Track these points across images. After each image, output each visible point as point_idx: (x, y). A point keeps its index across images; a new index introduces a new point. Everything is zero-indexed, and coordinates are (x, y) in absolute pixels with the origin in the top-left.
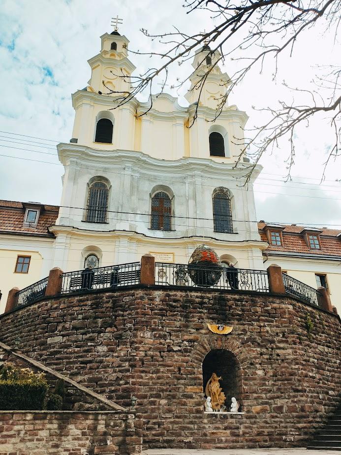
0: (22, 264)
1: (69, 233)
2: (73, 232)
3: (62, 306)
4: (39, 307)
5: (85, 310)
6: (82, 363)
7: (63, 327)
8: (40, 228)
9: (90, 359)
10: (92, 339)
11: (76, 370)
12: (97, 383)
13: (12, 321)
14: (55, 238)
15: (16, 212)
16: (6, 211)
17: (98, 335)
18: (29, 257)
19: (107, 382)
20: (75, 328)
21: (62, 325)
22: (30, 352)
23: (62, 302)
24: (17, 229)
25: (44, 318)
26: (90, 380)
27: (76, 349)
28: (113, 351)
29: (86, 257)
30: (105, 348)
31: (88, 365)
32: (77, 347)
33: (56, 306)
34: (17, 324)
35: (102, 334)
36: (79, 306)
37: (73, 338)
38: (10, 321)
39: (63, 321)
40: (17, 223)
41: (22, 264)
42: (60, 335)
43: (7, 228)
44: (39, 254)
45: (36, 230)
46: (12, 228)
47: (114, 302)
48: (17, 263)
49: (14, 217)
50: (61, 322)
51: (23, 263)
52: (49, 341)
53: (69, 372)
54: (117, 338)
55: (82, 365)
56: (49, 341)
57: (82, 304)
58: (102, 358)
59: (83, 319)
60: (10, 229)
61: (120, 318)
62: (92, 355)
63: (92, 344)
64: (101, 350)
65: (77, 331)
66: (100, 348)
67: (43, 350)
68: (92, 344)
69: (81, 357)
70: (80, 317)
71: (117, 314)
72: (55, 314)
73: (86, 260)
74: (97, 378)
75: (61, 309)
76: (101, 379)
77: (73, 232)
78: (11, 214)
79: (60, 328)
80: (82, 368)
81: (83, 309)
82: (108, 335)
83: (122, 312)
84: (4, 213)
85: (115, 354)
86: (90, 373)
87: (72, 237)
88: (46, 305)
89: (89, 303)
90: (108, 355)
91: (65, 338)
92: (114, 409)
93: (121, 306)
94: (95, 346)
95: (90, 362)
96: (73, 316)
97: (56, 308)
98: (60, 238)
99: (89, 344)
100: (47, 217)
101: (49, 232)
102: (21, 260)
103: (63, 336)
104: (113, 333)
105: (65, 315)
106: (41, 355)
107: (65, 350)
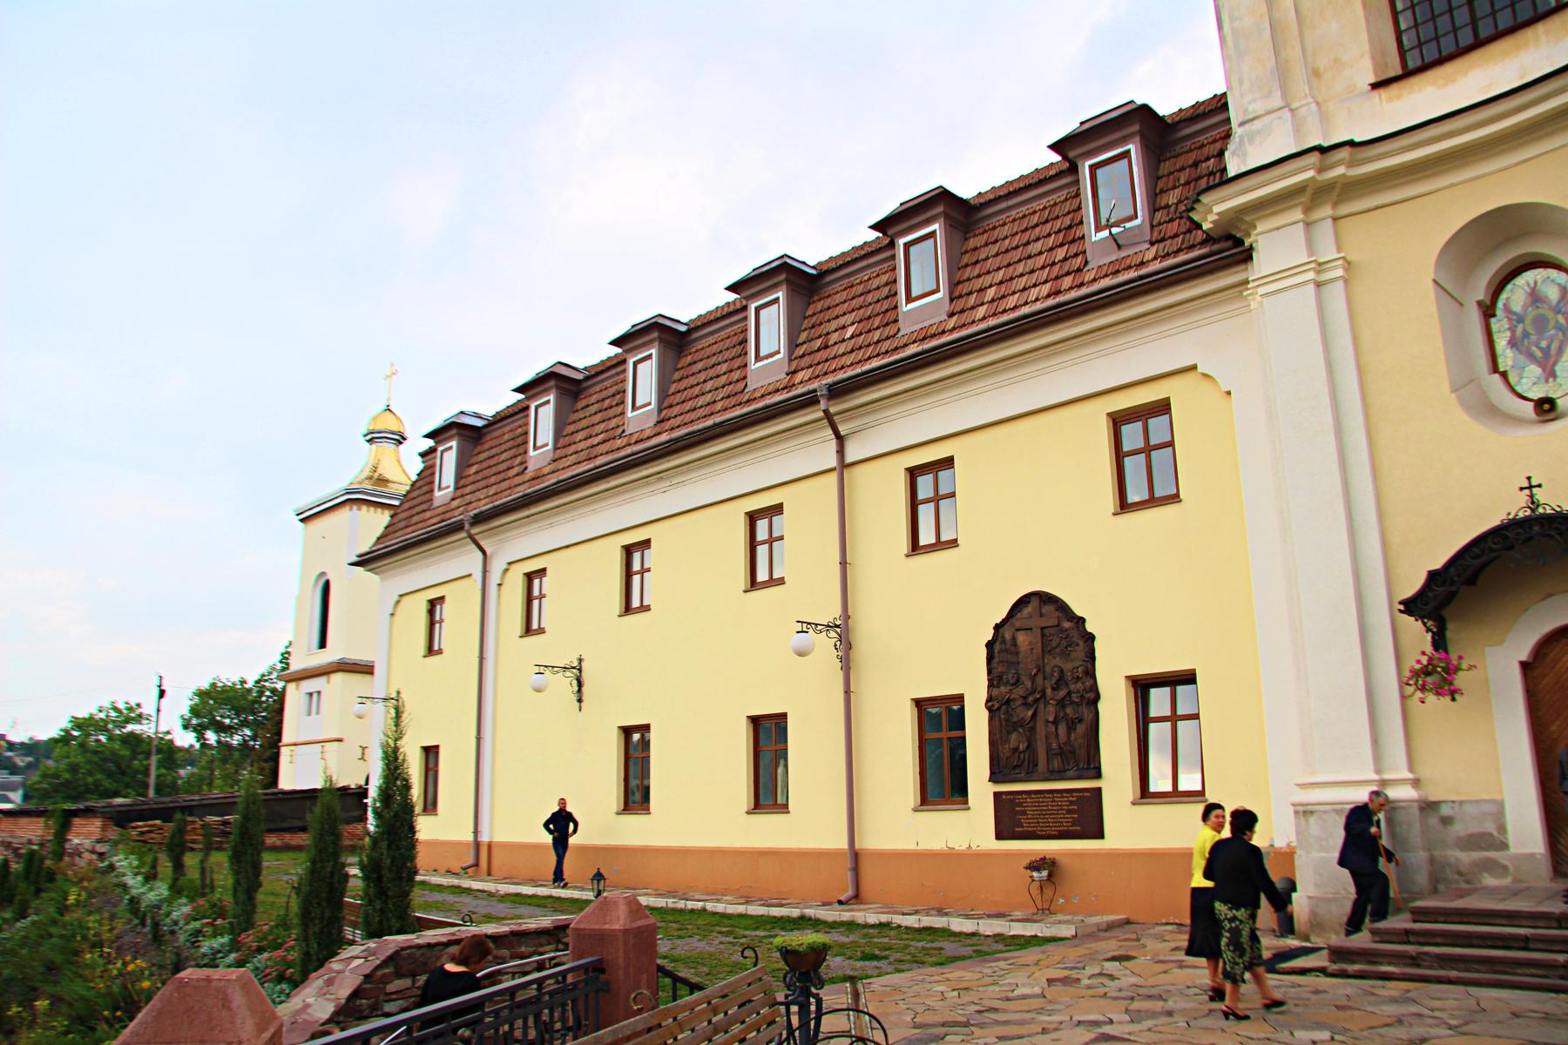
1: (1312, 196)
2: (1338, 180)
14: (1246, 256)
18: (1163, 407)
24: (1067, 282)
29: (1480, 292)
44: (1205, 375)
46: (1046, 289)
48: (1119, 456)
51: (1148, 449)
60: (1038, 300)
73: (1488, 311)
77: (1338, 180)
87: (1344, 209)
98: (1277, 247)
101: (1209, 239)
102: (1132, 435)
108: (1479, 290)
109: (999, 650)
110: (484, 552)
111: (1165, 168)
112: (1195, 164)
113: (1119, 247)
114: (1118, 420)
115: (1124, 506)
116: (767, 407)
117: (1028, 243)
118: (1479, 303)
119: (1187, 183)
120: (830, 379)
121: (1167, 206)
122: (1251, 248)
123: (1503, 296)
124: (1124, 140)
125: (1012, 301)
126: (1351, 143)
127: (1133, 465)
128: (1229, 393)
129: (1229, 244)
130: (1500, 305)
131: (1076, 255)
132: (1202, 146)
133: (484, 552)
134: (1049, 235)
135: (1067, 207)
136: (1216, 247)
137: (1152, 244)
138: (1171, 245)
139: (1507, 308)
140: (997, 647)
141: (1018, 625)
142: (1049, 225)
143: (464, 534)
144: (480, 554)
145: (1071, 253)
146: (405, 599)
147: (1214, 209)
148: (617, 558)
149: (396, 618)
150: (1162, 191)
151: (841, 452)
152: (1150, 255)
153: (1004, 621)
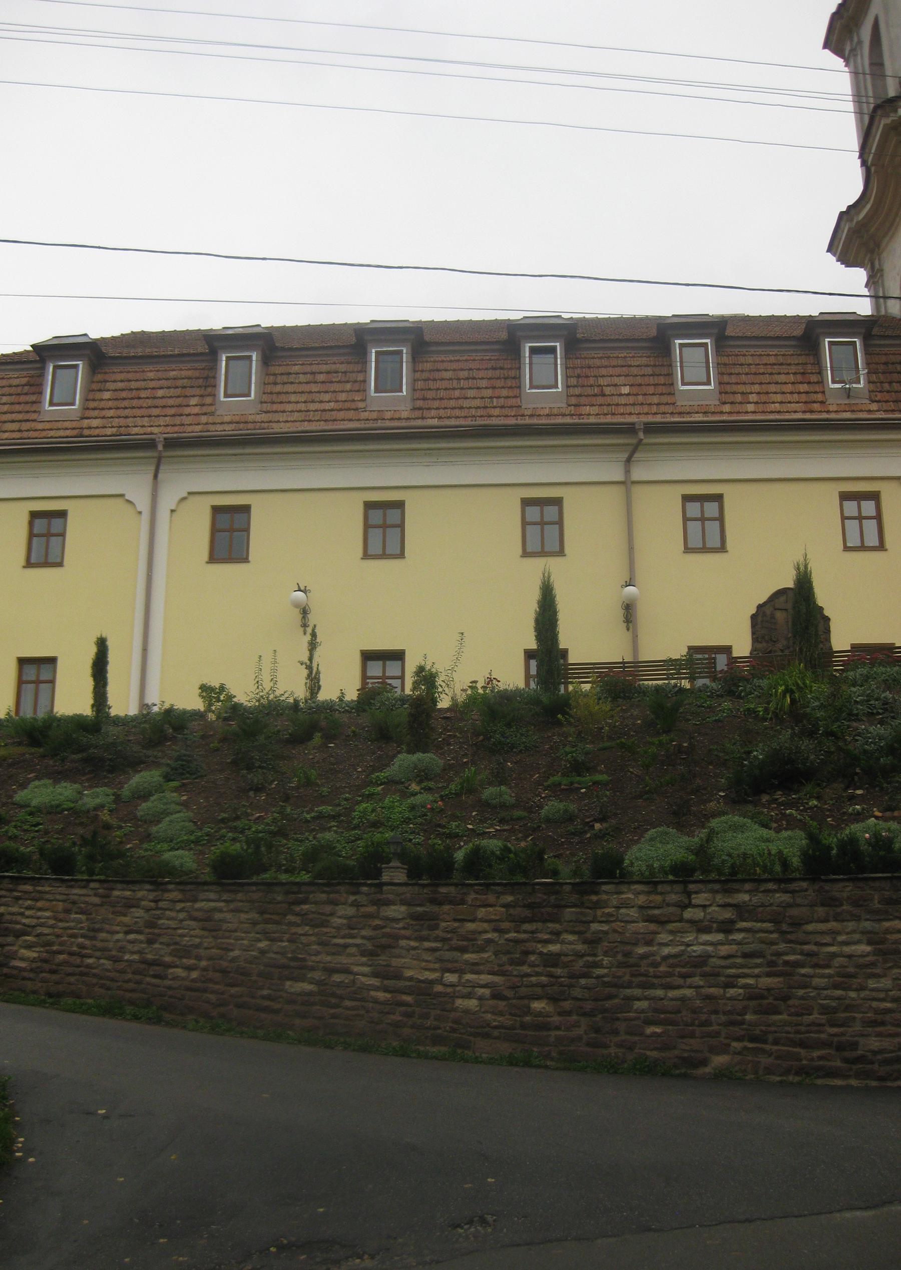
15: (783, 351)
16: (752, 351)
24: (816, 406)
40: (804, 388)
43: (784, 407)
45: (874, 406)
49: (784, 369)
78: (772, 360)
84: (749, 360)
100: (884, 359)
109: (762, 620)
112: (886, 364)
113: (849, 397)
114: (845, 497)
116: (563, 424)
120: (650, 419)
138: (885, 406)
140: (760, 619)
141: (777, 606)
143: (155, 454)
146: (193, 499)
149: (175, 514)
151: (627, 472)
153: (765, 604)
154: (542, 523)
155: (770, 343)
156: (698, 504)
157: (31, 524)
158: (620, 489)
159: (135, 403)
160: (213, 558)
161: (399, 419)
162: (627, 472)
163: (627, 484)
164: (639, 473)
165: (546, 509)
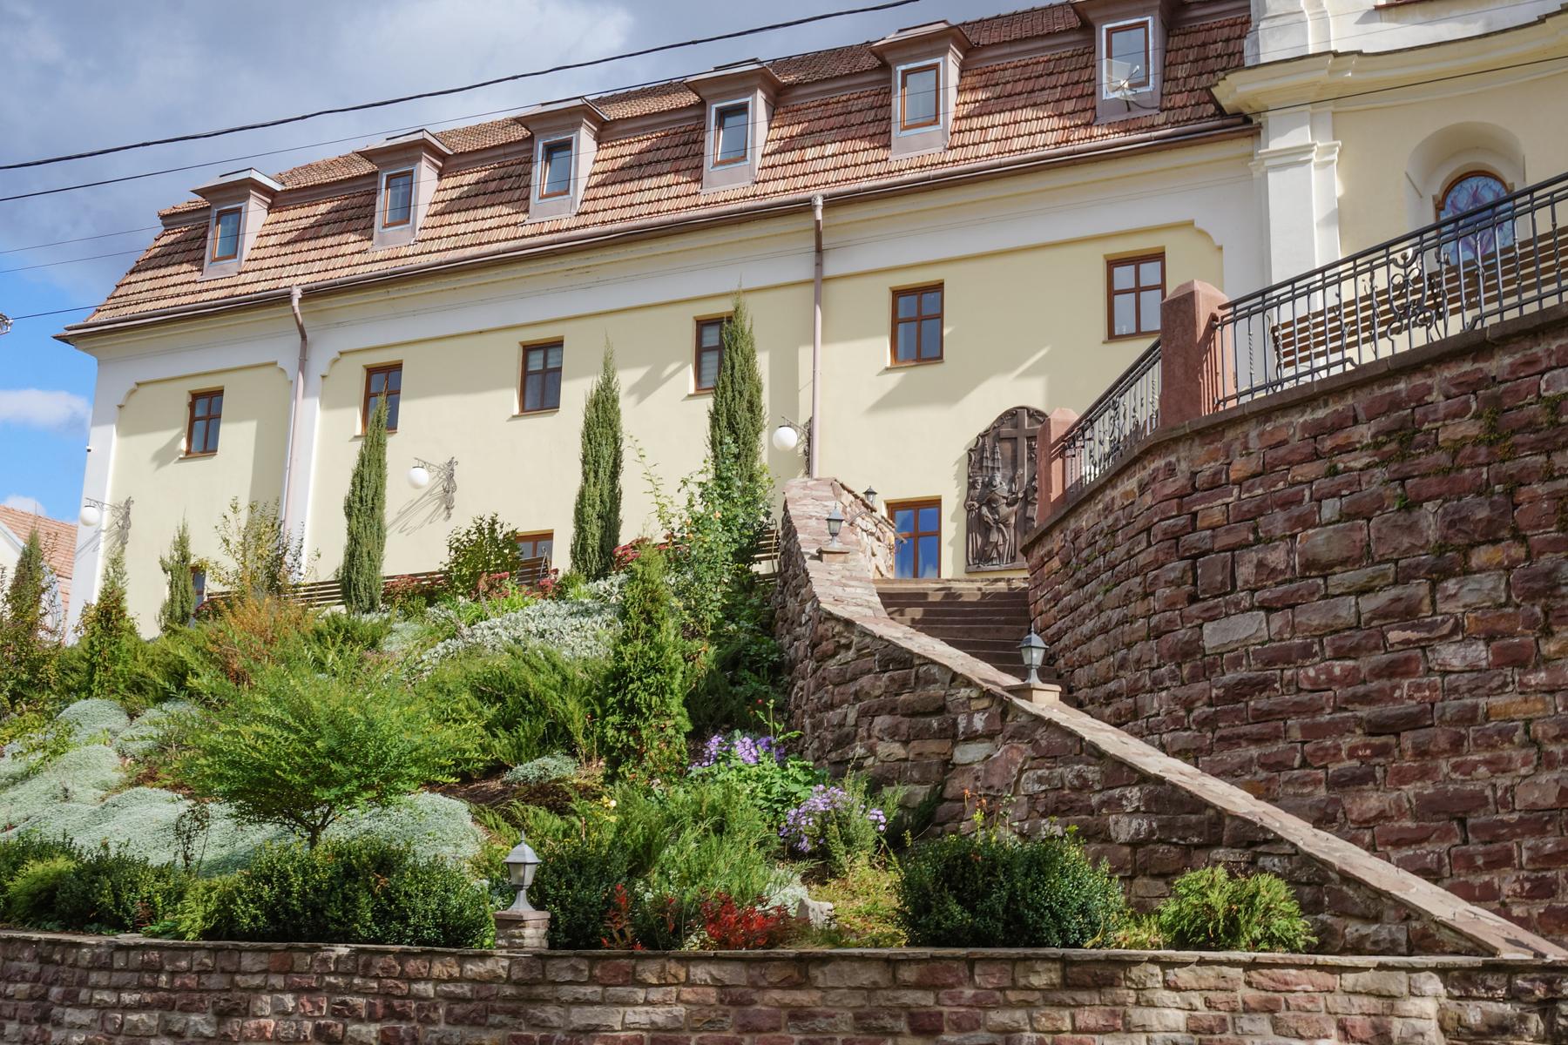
0: (1133, 296)
3: (1240, 467)
4: (1143, 488)
5: (1348, 470)
6: (1375, 728)
7: (1261, 564)
8: (1179, 100)
9: (1411, 706)
10: (1406, 614)
11: (1355, 763)
12: (1462, 822)
13: (1065, 564)
15: (1060, 52)
17: (1433, 590)
19: (1515, 816)
20: (1309, 565)
21: (1253, 556)
22: (1142, 689)
23: (1237, 446)
25: (1175, 536)
26: (1427, 808)
27: (1337, 668)
28: (1520, 660)
30: (1480, 652)
31: (1408, 740)
32: (1338, 657)
33: (1208, 469)
34: (1080, 575)
35: (1451, 585)
36: (1316, 456)
37: (1313, 616)
38: (1055, 563)
39: (1258, 541)
41: (1133, 296)
42: (1252, 608)
45: (1162, 118)
47: (1496, 409)
48: (1111, 293)
49: (1053, 80)
50: (1247, 546)
52: (1213, 636)
53: (1321, 774)
54: (1531, 596)
55: (1376, 741)
56: (1213, 636)
57: (1329, 444)
58: (1468, 701)
59: (1346, 516)
61: (1539, 489)
62: (1419, 688)
63: (1409, 634)
64: (1457, 663)
65: (1325, 577)
66: (1452, 655)
67: (1194, 678)
68: (1409, 634)
69: (1366, 699)
70: (1330, 508)
71: (1510, 467)
72: (1213, 510)
74: (1460, 797)
75: (1239, 483)
76: (1479, 801)
79: (1245, 572)
80: (1383, 751)
81: (1341, 466)
82: (1488, 582)
83: (1542, 459)
85: (1532, 679)
86: (1424, 774)
88: (1171, 470)
89: (1364, 433)
90: (1495, 684)
91: (1278, 620)
92: (1479, 947)
93: (1530, 425)
94: (1424, 646)
95: (1413, 722)
96: (1295, 511)
97: (1215, 485)
99: (1394, 636)
100: (1202, 37)
102: (1124, 277)
103: (1269, 608)
104: (1508, 569)
105: (1260, 511)
106: (1189, 705)
107: (1288, 673)
108: (1437, 189)
110: (304, 337)
111: (1176, 42)
112: (1204, 45)
115: (1112, 336)
117: (1033, 91)
118: (1434, 198)
119: (1196, 61)
121: (1176, 79)
122: (1260, 126)
123: (1452, 195)
124: (1145, 12)
125: (1017, 143)
126: (1359, 53)
127: (1124, 304)
128: (1221, 248)
129: (1240, 120)
130: (1449, 201)
131: (1085, 110)
132: (1211, 29)
133: (304, 337)
134: (1055, 87)
135: (1073, 63)
136: (1226, 122)
137: (1162, 110)
139: (1453, 205)
142: (1054, 78)
144: (298, 337)
145: (1079, 107)
147: (1233, 91)
148: (517, 353)
150: (1171, 64)
151: (819, 264)
152: (1162, 118)
154: (1138, 290)
155: (1006, 50)
156: (1132, 268)
157: (192, 406)
158: (810, 290)
159: (800, 168)
160: (525, 410)
161: (558, 231)
162: (819, 264)
163: (819, 282)
164: (831, 269)
165: (1144, 267)
